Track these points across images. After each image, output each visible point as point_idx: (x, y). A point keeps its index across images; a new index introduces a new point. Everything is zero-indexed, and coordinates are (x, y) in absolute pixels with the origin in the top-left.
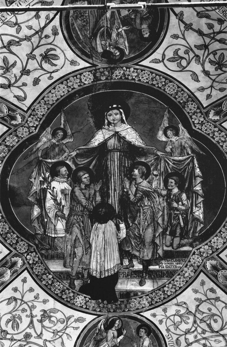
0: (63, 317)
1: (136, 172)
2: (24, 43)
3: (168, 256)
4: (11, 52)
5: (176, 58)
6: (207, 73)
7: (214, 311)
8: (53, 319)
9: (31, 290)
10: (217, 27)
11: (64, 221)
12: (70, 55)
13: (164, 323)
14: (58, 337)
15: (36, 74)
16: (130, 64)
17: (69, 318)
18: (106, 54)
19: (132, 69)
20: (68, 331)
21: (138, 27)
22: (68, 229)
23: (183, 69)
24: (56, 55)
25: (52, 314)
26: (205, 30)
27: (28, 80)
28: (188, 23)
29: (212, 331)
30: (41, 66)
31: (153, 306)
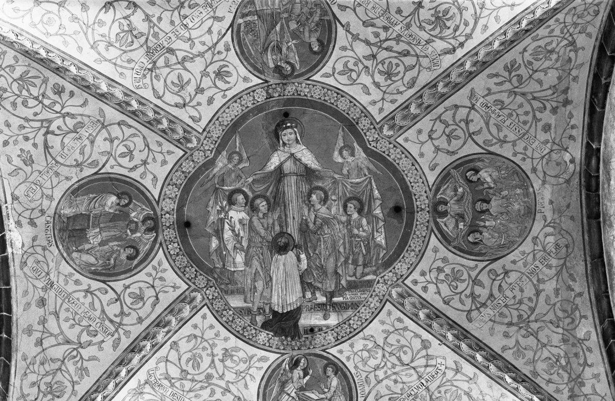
0: (245, 356)
1: (314, 197)
2: (198, 59)
3: (352, 286)
4: (185, 69)
5: (347, 71)
6: (377, 85)
7: (403, 342)
8: (235, 358)
9: (212, 327)
10: (383, 35)
11: (243, 254)
12: (243, 71)
13: (351, 360)
14: (240, 378)
15: (208, 93)
16: (301, 79)
17: (252, 357)
18: (278, 69)
19: (304, 85)
20: (251, 371)
21: (307, 40)
22: (247, 263)
23: (353, 82)
24: (228, 72)
25: (234, 353)
26: (373, 40)
27: (202, 98)
28: (355, 33)
29: (403, 364)
30: (215, 84)
31: (339, 341)
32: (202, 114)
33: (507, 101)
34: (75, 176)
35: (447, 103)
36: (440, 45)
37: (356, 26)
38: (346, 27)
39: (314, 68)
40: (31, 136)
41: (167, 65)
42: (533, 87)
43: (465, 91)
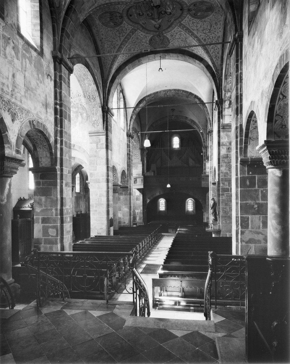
6: (139, 36)
12: (168, 36)
15: (174, 33)
32: (176, 29)
33: (113, 40)
34: (206, 19)
35: (125, 37)
36: (129, 46)
37: (145, 44)
38: (147, 43)
39: (153, 37)
41: (183, 39)
42: (109, 43)
43: (122, 40)
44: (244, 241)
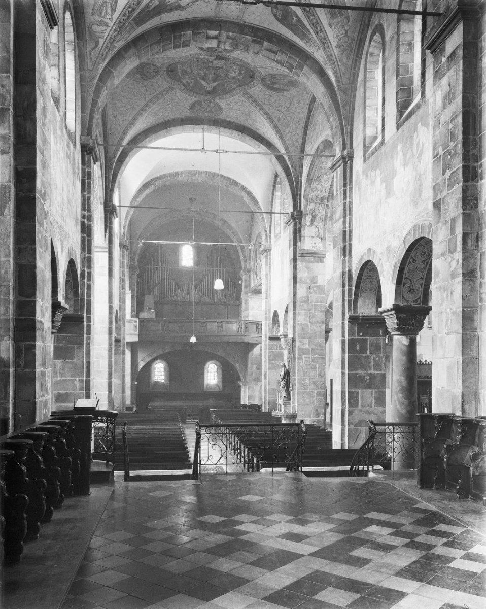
27: (236, 101)
35: (153, 96)
40: (294, 108)
43: (147, 100)
44: (352, 423)
